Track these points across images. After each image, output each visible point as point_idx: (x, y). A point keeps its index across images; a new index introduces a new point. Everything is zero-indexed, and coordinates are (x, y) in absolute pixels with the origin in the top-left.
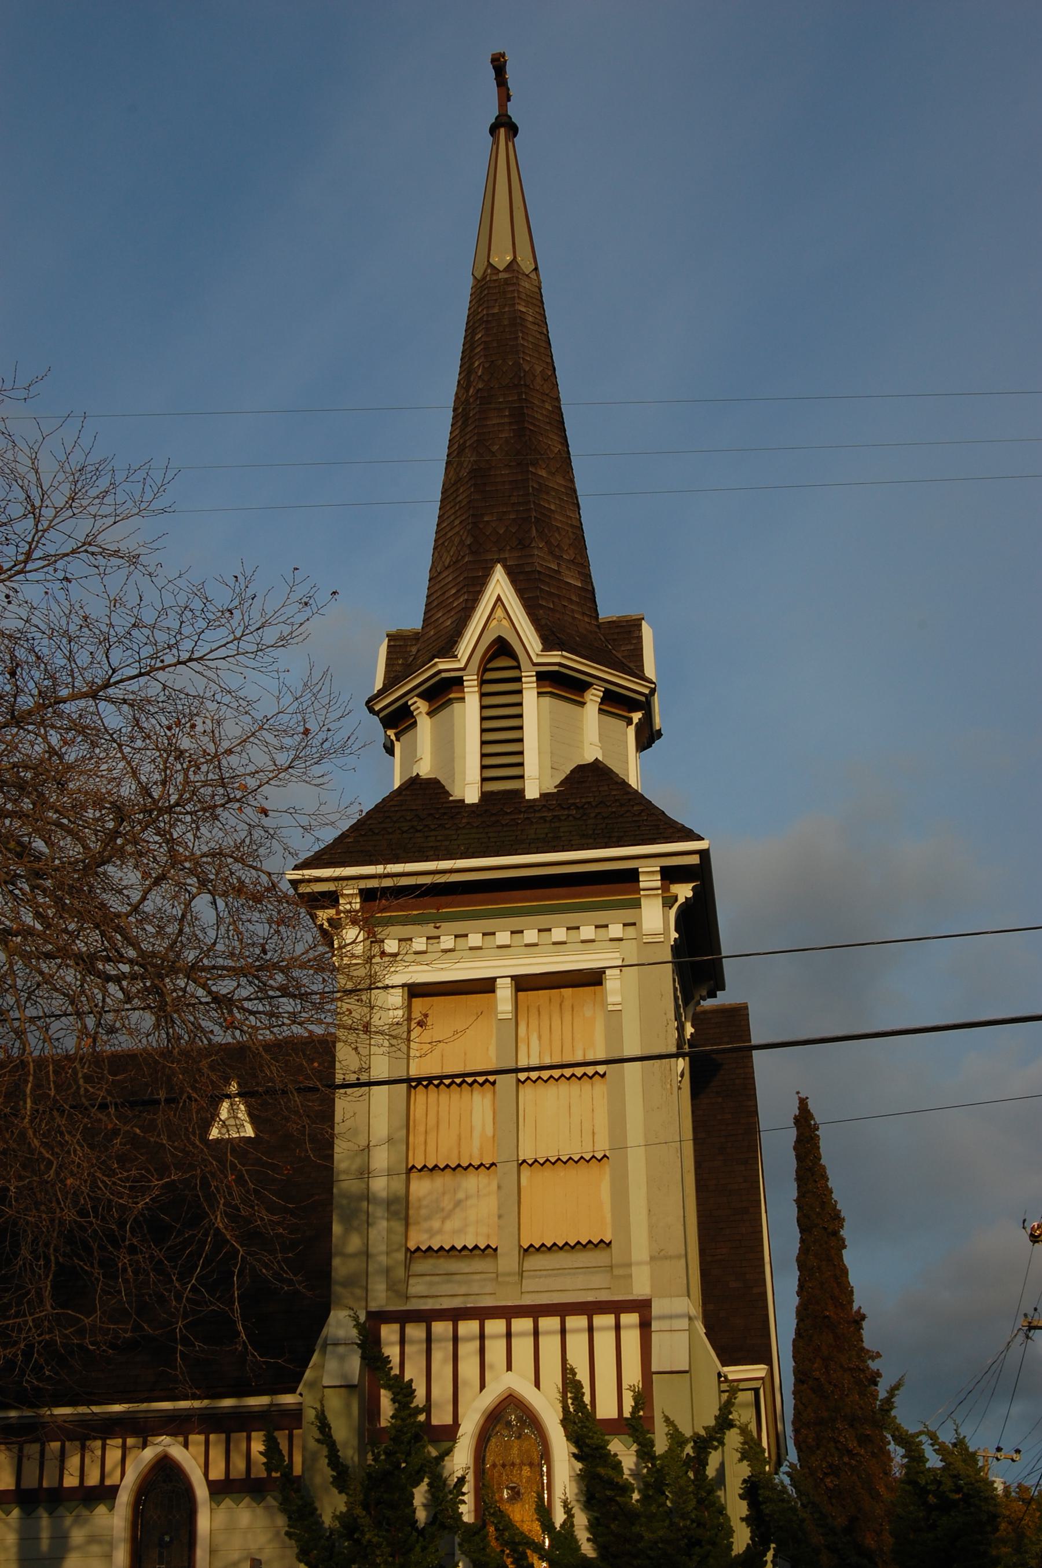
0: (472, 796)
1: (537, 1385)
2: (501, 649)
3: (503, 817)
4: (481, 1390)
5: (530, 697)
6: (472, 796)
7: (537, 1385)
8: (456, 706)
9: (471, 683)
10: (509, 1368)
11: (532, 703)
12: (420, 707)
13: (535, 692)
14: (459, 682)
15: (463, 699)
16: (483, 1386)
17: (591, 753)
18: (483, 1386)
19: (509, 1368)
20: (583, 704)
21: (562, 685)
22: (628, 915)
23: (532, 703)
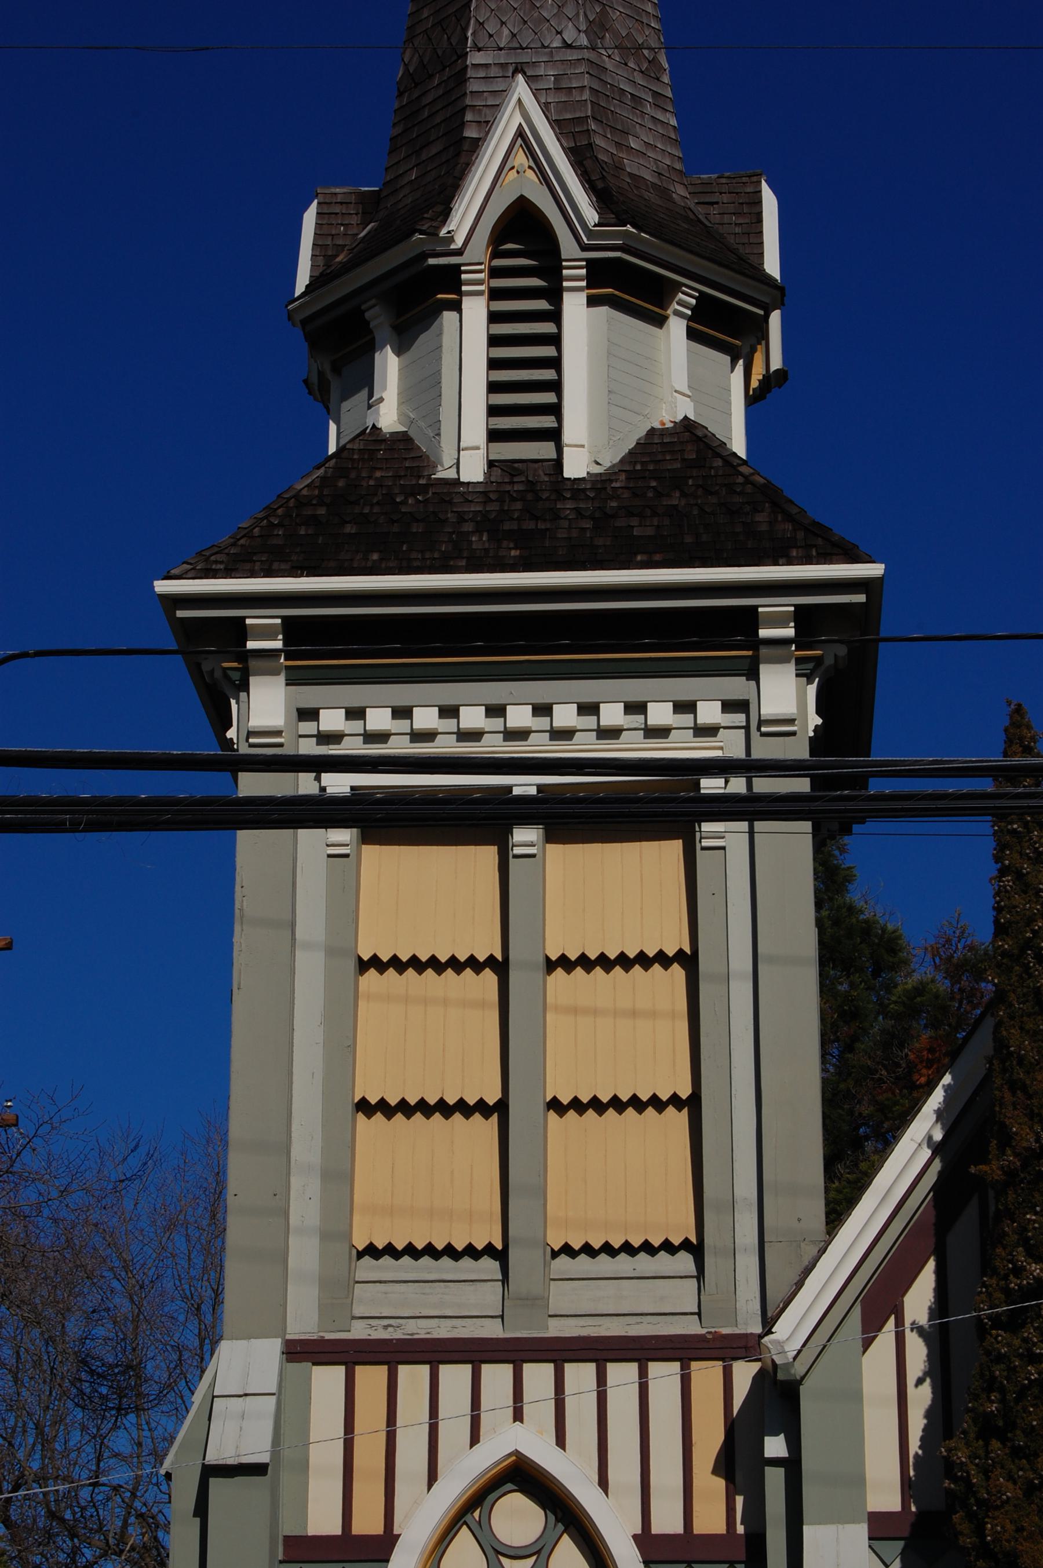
0: (473, 470)
1: (561, 1441)
2: (522, 228)
3: (529, 509)
4: (471, 1446)
5: (575, 306)
6: (473, 470)
7: (561, 1441)
8: (449, 317)
9: (476, 278)
10: (518, 1416)
11: (579, 318)
12: (378, 317)
13: (582, 298)
14: (450, 279)
15: (456, 307)
16: (475, 1439)
17: (674, 407)
18: (475, 1439)
19: (518, 1416)
20: (660, 321)
21: (630, 289)
22: (736, 687)
23: (579, 318)
